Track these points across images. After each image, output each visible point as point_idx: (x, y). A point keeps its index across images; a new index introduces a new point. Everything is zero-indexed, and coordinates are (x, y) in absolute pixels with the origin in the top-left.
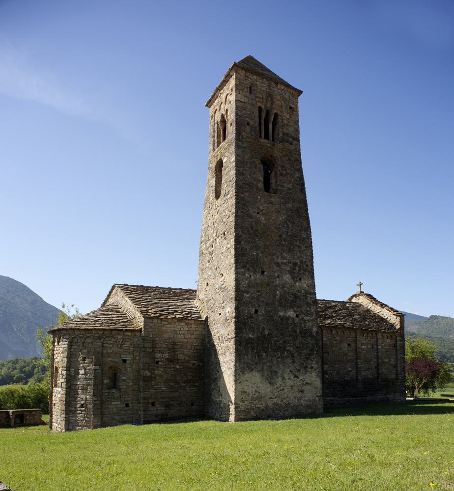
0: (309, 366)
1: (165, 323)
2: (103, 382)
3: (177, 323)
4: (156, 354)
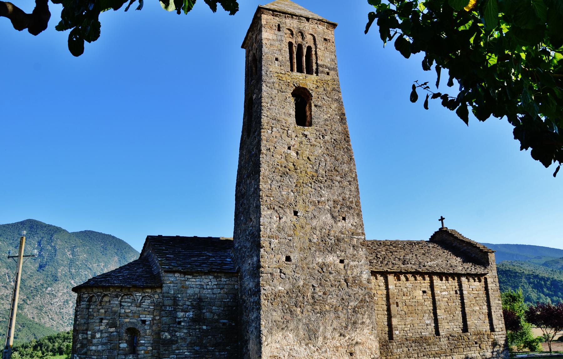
0: (360, 322)
1: (190, 277)
2: (119, 347)
3: (203, 277)
4: (178, 313)
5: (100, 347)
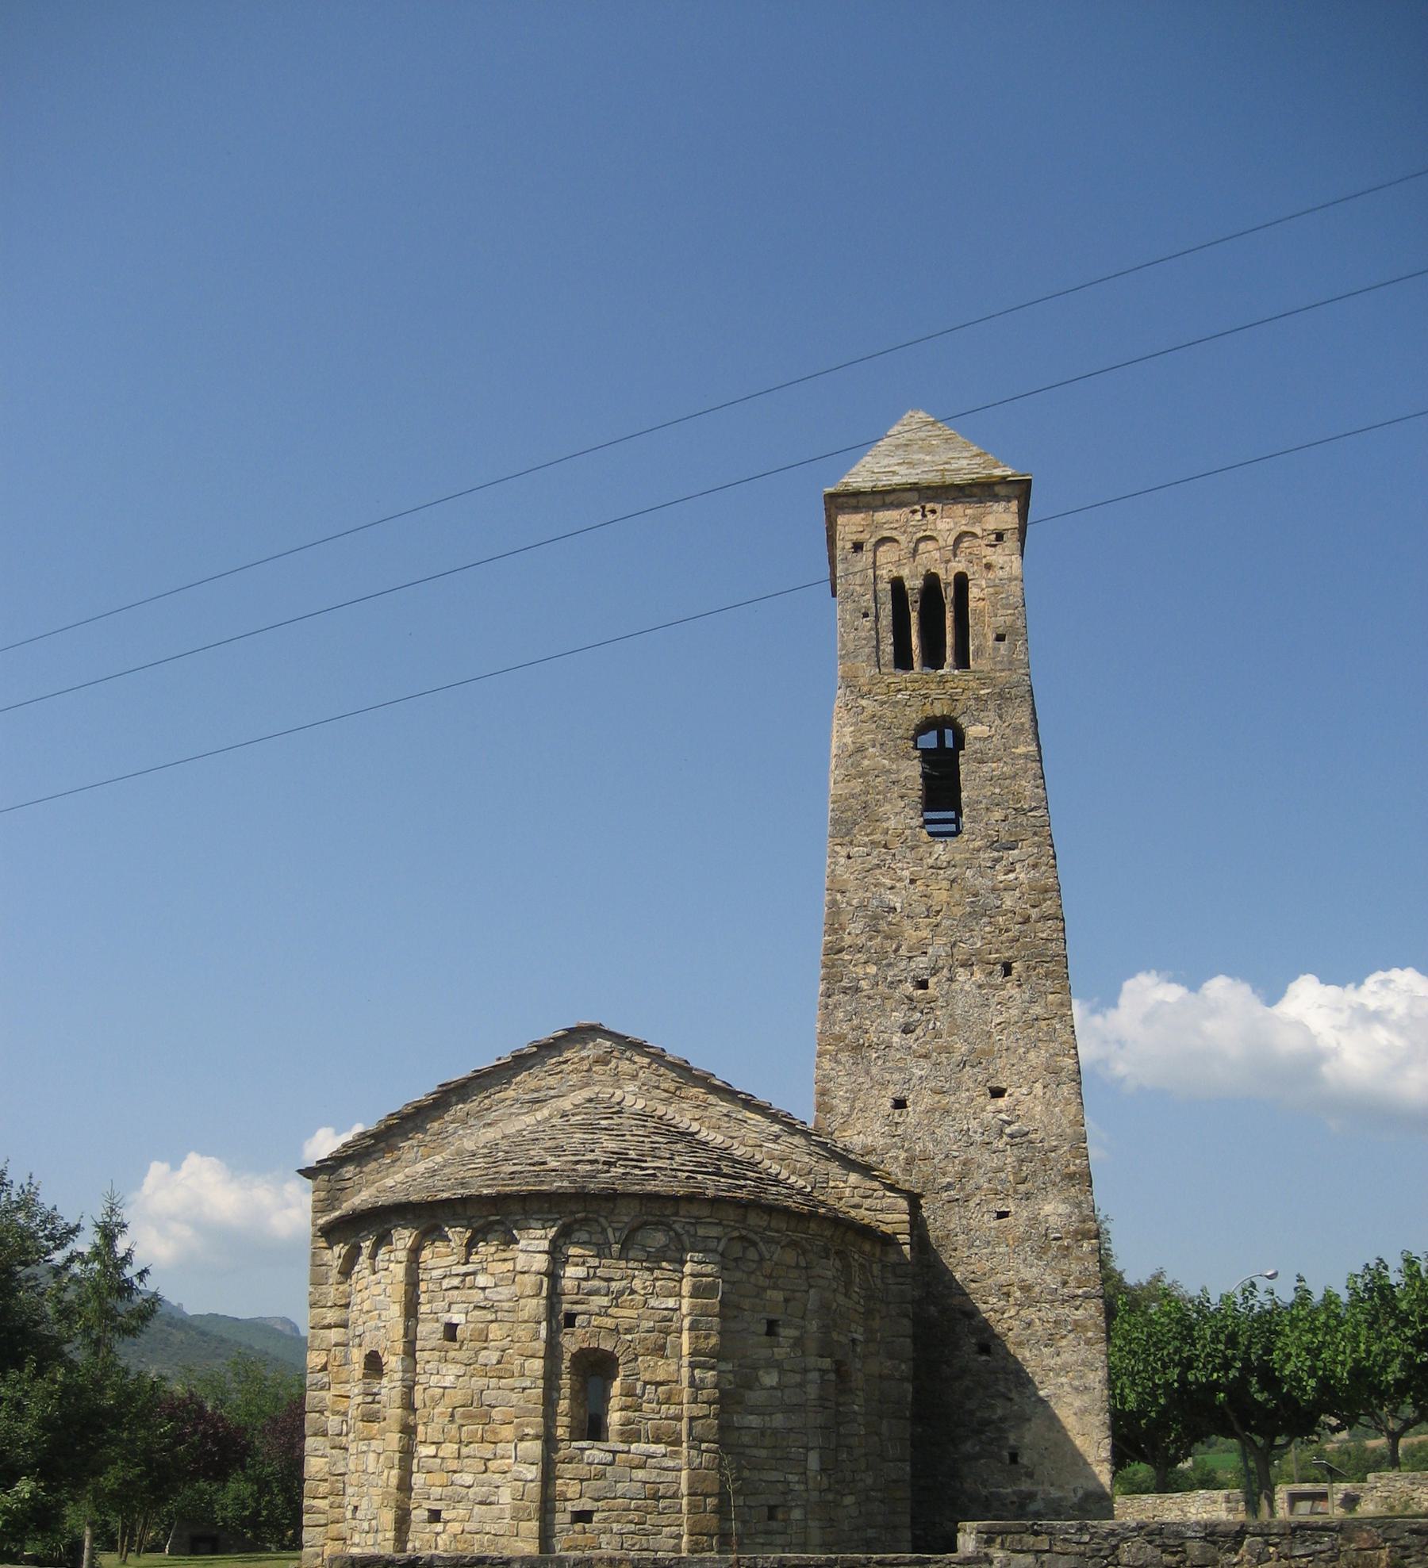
5: (778, 1420)
